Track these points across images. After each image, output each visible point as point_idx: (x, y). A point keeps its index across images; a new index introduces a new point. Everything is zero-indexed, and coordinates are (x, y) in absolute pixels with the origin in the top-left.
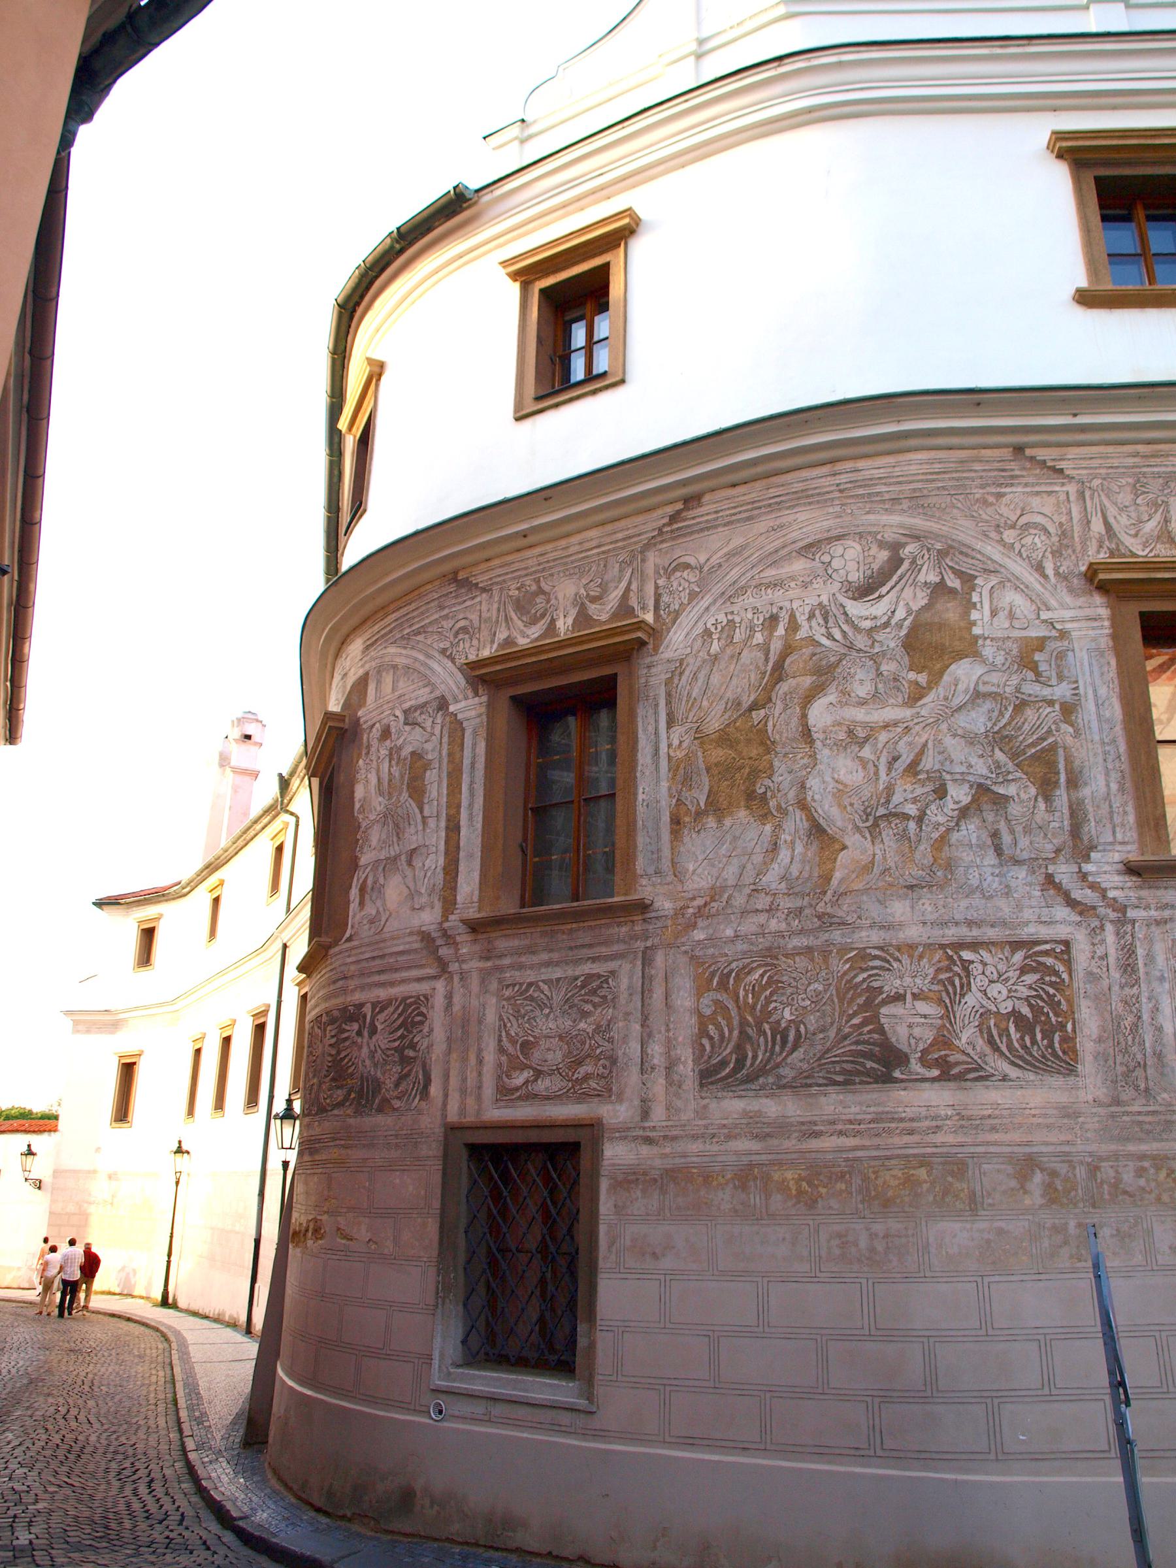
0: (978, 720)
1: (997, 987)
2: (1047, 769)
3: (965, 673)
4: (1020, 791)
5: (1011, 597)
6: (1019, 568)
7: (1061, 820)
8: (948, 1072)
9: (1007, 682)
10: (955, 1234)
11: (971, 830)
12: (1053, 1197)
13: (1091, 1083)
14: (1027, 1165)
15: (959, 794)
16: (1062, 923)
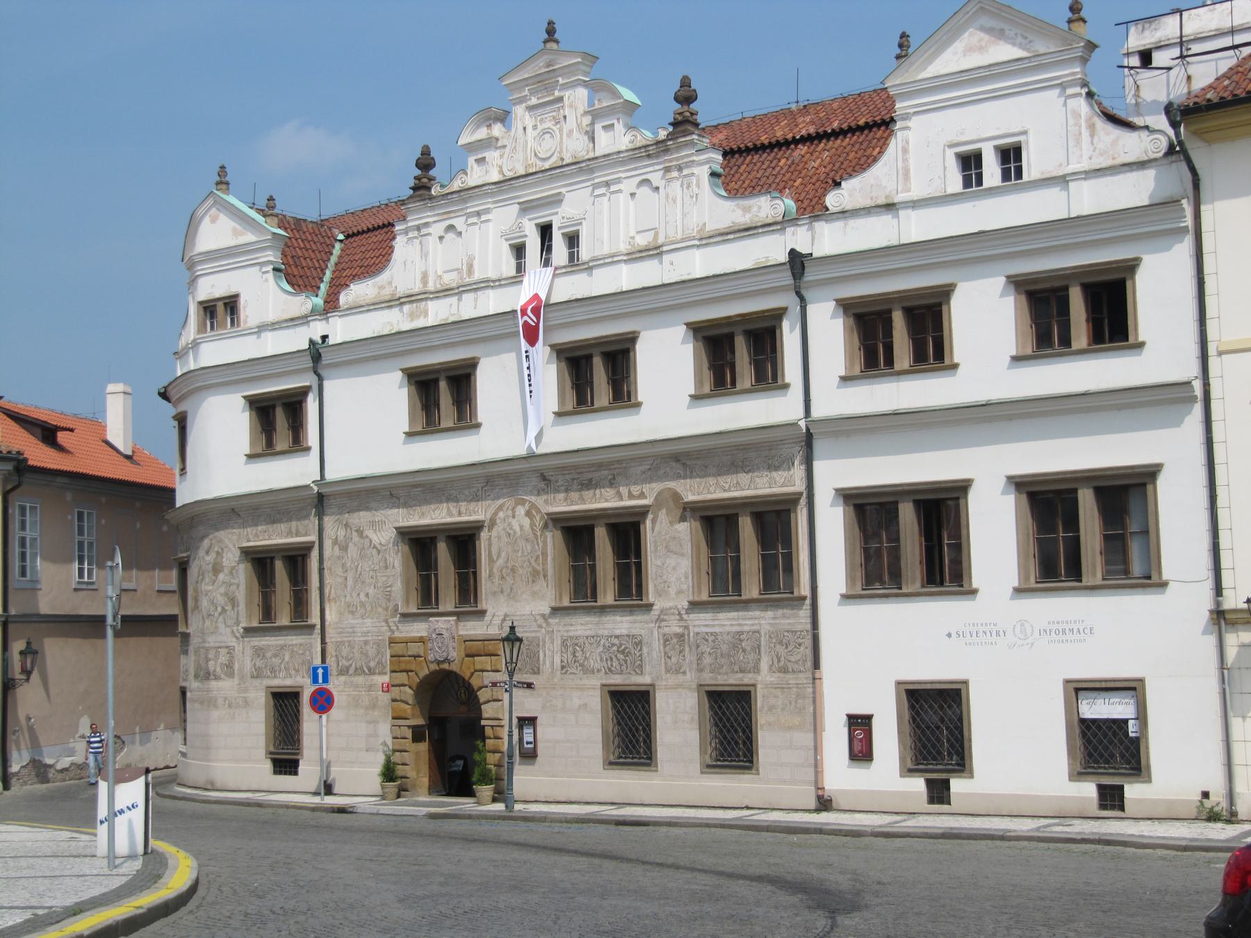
0: (222, 590)
1: (223, 659)
2: (233, 601)
3: (221, 576)
4: (228, 608)
5: (230, 555)
6: (231, 546)
7: (234, 616)
8: (217, 678)
9: (227, 579)
10: (215, 714)
11: (221, 619)
12: (230, 706)
13: (236, 681)
14: (226, 699)
15: (219, 609)
16: (232, 642)
